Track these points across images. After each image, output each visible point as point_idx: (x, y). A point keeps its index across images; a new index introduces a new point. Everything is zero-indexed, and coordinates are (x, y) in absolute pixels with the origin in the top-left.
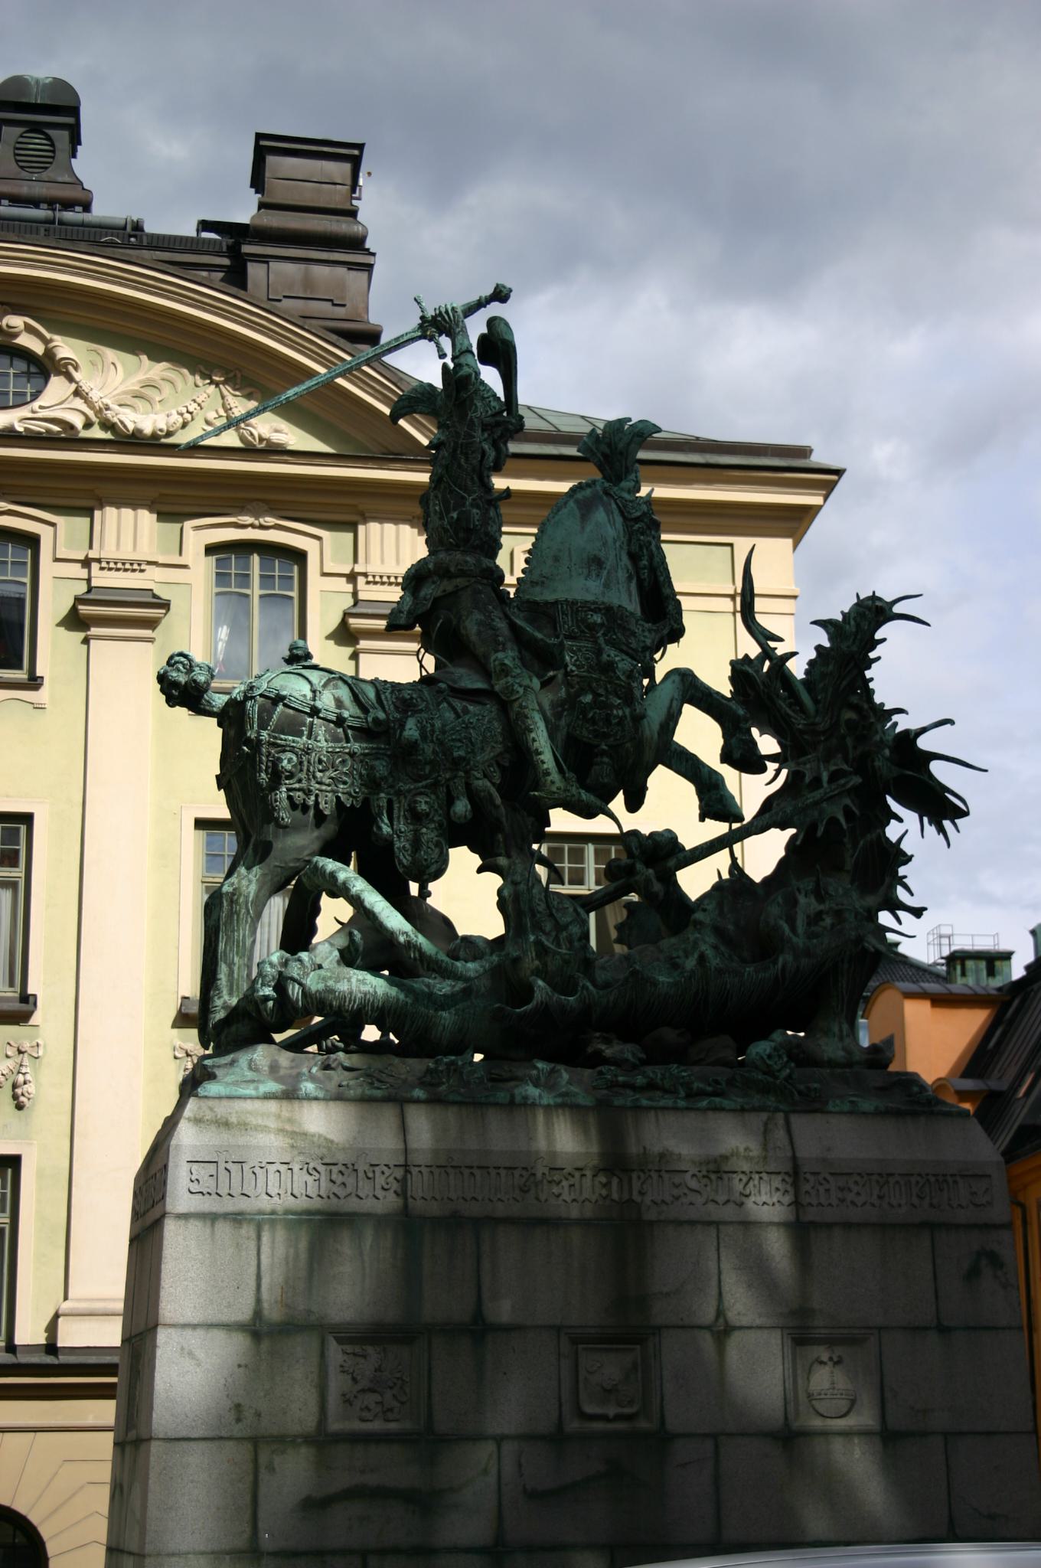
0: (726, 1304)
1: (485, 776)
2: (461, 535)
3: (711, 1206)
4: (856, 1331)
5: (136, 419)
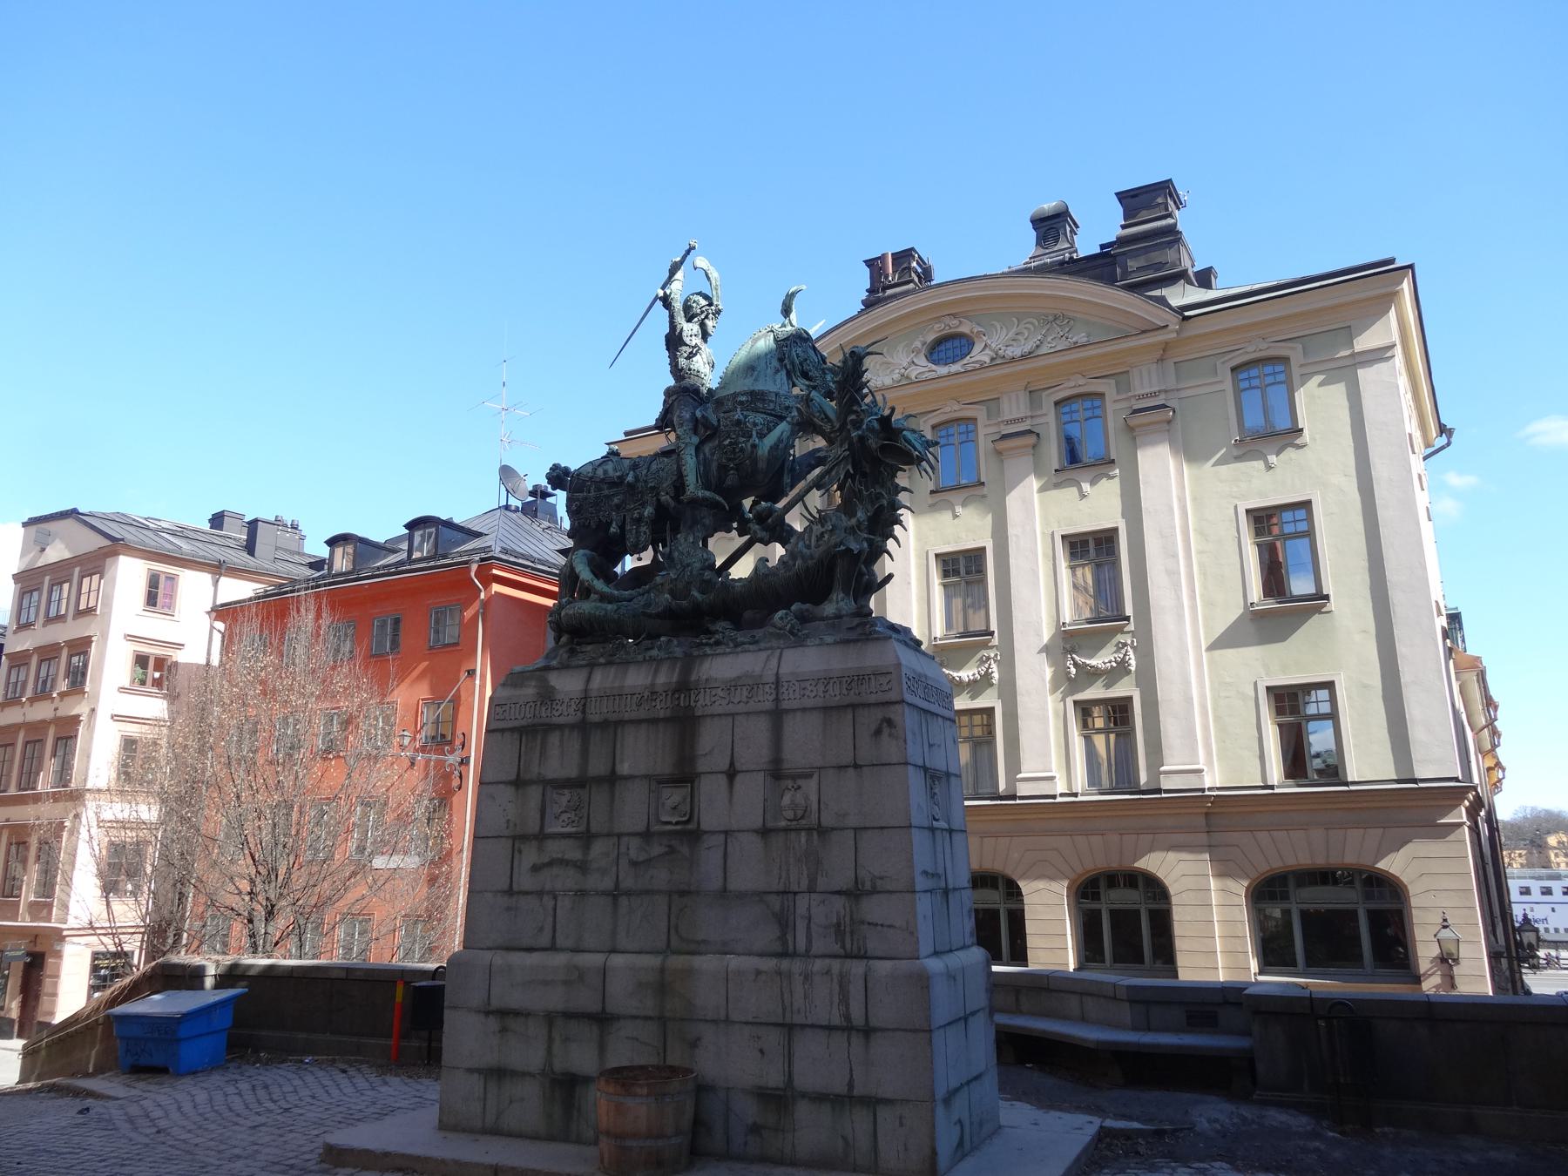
3: (730, 705)
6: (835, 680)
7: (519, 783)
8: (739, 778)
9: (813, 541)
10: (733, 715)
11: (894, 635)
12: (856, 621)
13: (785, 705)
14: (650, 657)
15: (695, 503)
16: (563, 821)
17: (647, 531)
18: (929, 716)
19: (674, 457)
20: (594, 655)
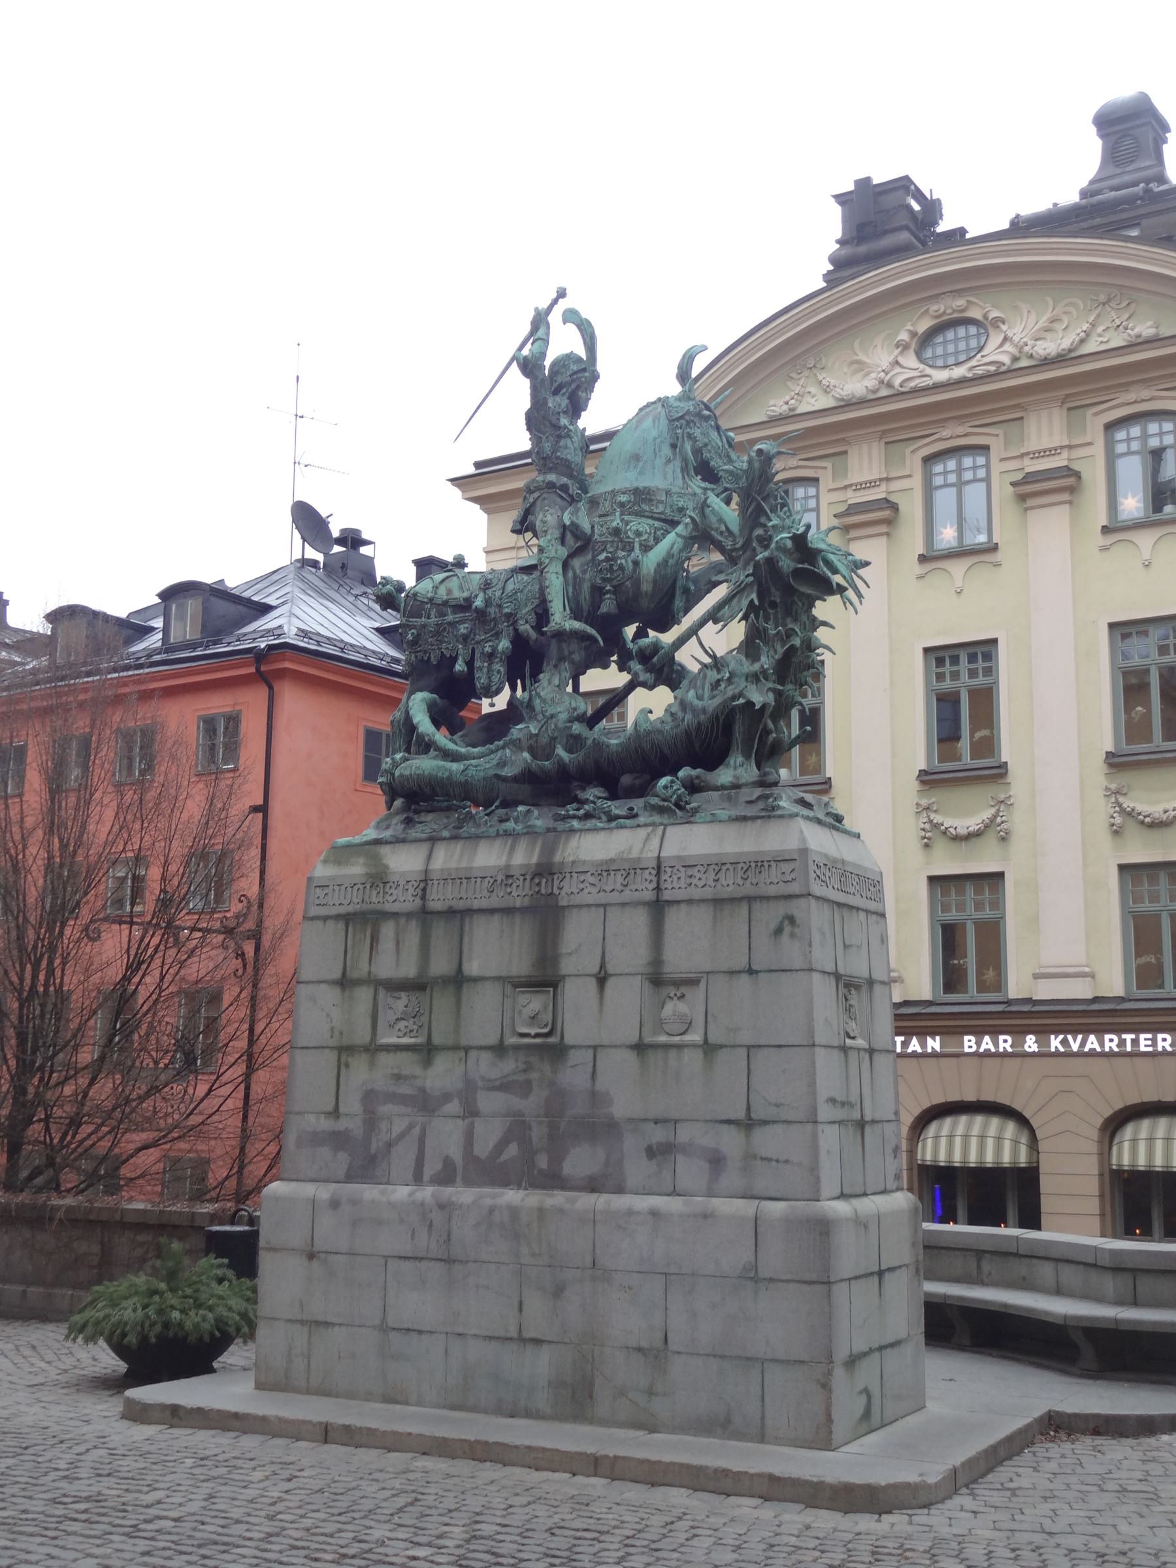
0: (607, 959)
1: (527, 622)
2: (542, 462)
3: (602, 894)
4: (692, 975)
5: (1048, 347)
6: (728, 866)
7: (345, 983)
8: (611, 983)
9: (706, 689)
10: (605, 906)
11: (806, 812)
12: (758, 792)
13: (667, 895)
14: (505, 831)
15: (560, 635)
16: (399, 1030)
17: (502, 669)
18: (845, 911)
19: (536, 574)
20: (435, 827)
